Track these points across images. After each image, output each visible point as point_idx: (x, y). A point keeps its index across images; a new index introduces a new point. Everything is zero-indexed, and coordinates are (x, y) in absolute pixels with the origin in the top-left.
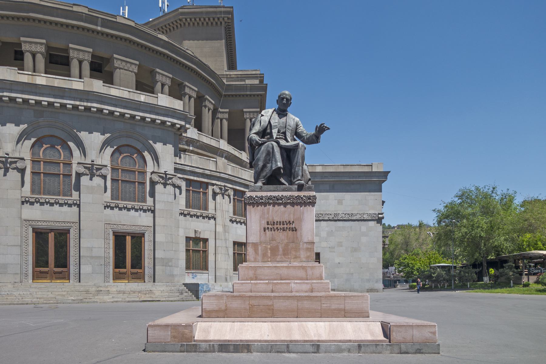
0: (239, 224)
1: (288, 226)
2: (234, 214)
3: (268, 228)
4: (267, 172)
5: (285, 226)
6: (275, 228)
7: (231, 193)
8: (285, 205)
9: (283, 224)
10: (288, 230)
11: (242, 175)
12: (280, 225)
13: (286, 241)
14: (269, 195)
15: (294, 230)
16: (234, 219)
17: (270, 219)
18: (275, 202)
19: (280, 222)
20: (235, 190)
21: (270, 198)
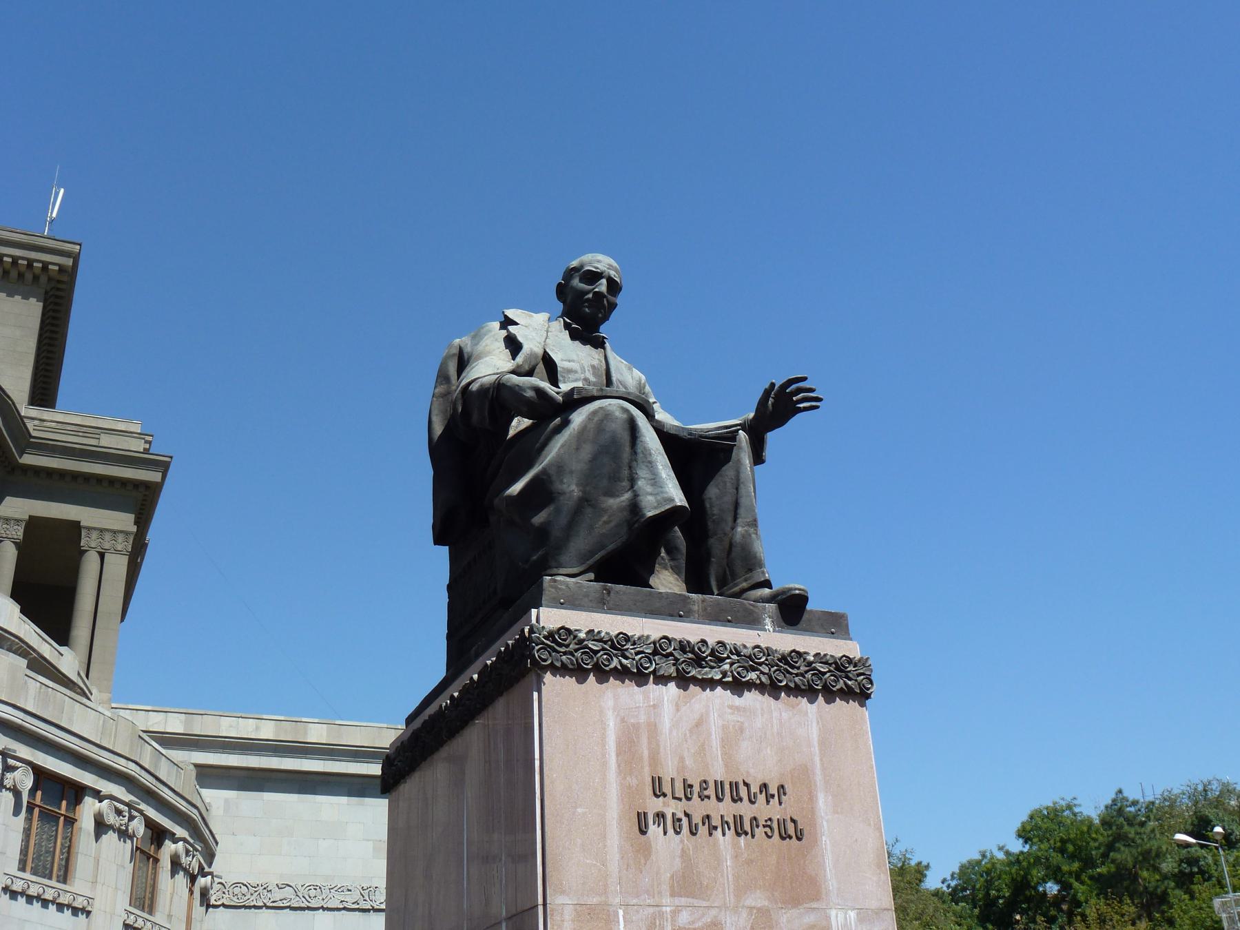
0: (37, 905)
1: (763, 810)
2: (22, 868)
3: (660, 816)
4: (603, 527)
5: (746, 810)
6: (697, 819)
7: (25, 780)
8: (738, 686)
9: (736, 799)
10: (759, 832)
11: (70, 720)
12: (719, 800)
13: (757, 899)
14: (655, 636)
15: (792, 832)
16: (18, 886)
17: (669, 771)
18: (690, 668)
19: (719, 785)
20: (42, 776)
21: (659, 649)
